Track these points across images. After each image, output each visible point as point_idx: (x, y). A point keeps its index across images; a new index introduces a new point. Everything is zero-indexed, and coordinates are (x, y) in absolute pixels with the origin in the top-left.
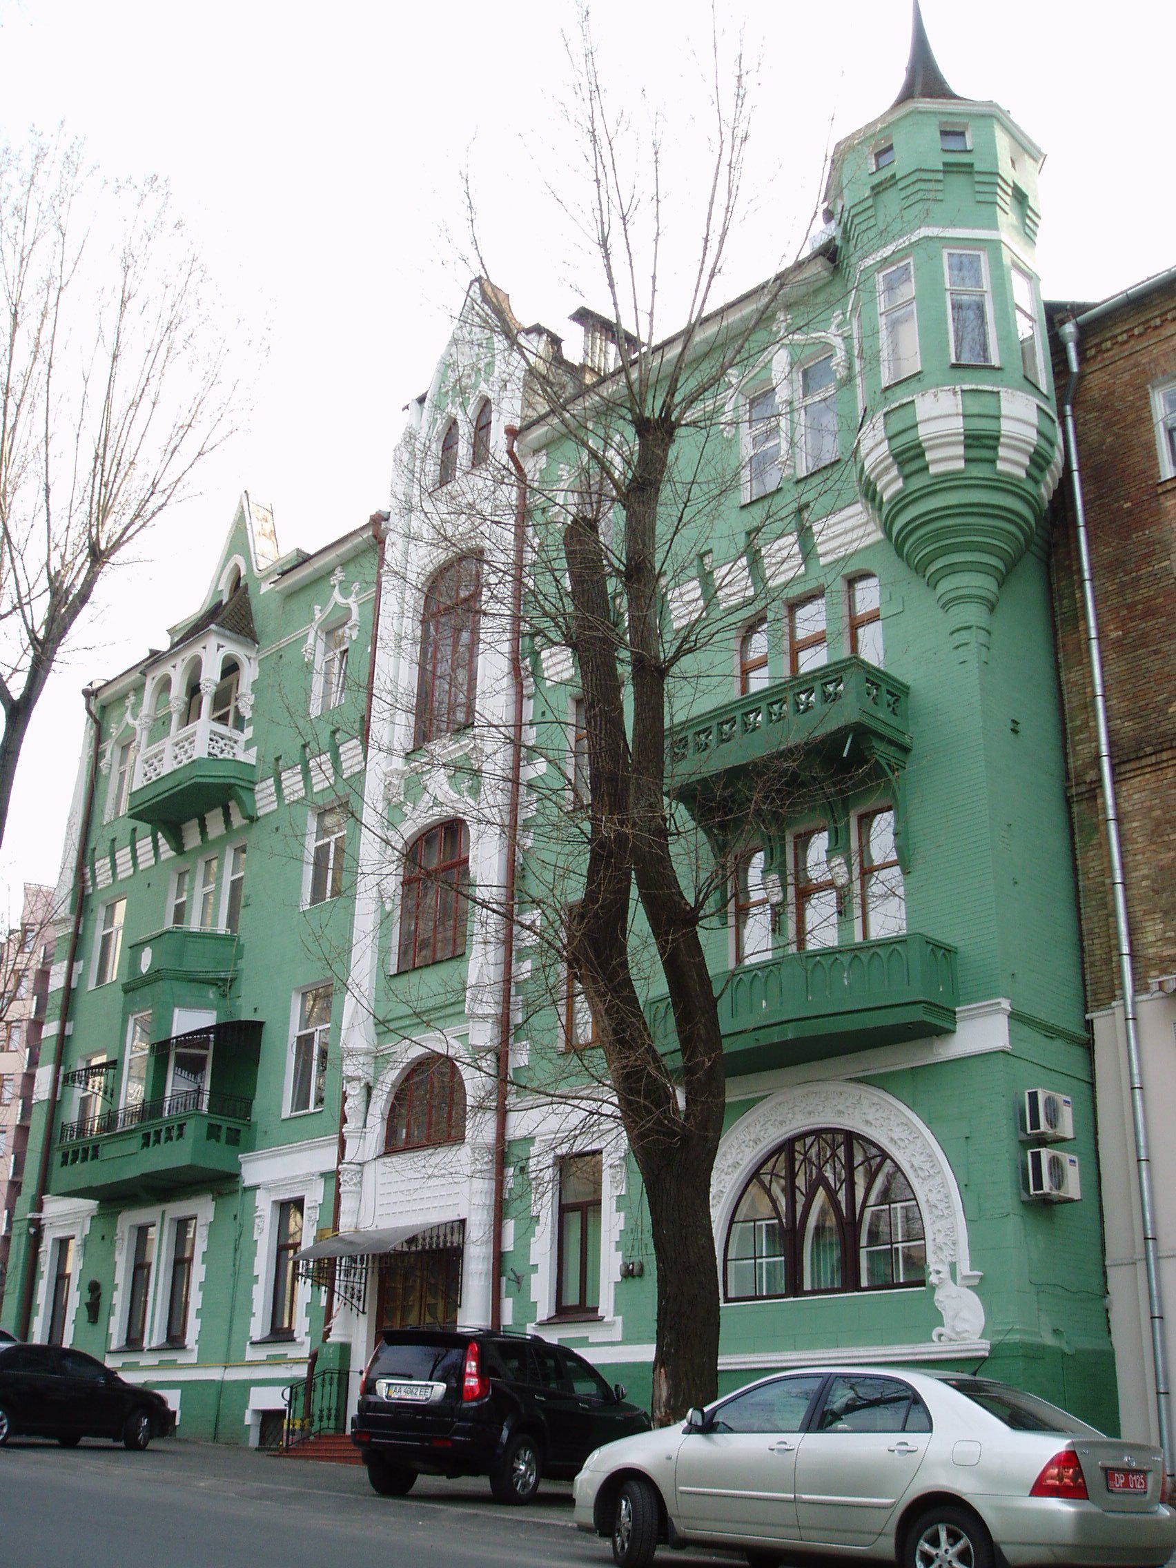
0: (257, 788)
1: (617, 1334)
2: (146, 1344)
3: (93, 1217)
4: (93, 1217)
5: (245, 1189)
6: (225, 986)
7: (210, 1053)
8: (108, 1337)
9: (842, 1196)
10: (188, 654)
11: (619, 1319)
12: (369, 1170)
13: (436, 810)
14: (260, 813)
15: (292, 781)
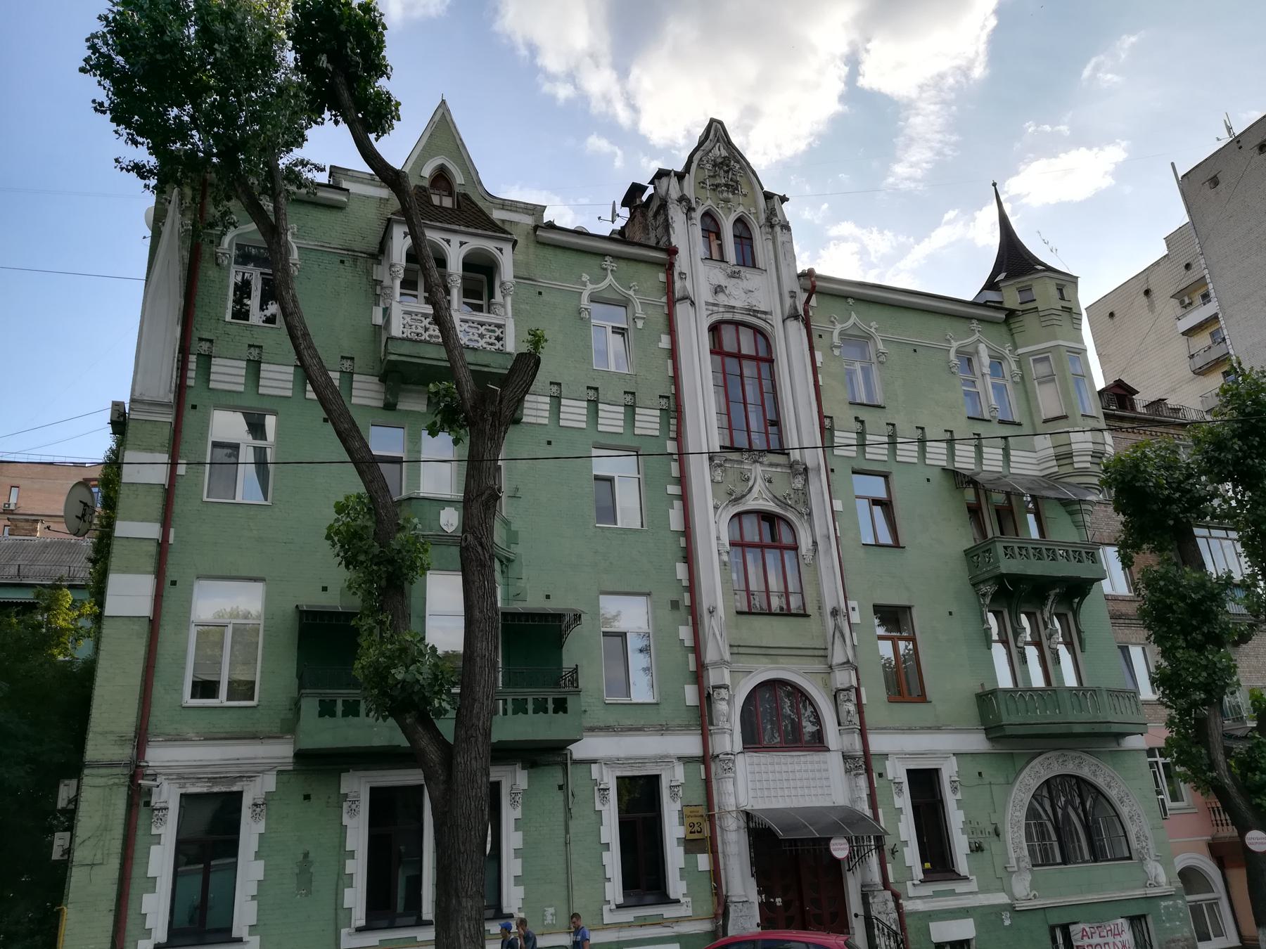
0: (527, 397)
1: (973, 886)
3: (280, 773)
4: (280, 773)
8: (340, 914)
9: (1080, 811)
10: (474, 243)
11: (973, 877)
13: (761, 501)
15: (574, 413)
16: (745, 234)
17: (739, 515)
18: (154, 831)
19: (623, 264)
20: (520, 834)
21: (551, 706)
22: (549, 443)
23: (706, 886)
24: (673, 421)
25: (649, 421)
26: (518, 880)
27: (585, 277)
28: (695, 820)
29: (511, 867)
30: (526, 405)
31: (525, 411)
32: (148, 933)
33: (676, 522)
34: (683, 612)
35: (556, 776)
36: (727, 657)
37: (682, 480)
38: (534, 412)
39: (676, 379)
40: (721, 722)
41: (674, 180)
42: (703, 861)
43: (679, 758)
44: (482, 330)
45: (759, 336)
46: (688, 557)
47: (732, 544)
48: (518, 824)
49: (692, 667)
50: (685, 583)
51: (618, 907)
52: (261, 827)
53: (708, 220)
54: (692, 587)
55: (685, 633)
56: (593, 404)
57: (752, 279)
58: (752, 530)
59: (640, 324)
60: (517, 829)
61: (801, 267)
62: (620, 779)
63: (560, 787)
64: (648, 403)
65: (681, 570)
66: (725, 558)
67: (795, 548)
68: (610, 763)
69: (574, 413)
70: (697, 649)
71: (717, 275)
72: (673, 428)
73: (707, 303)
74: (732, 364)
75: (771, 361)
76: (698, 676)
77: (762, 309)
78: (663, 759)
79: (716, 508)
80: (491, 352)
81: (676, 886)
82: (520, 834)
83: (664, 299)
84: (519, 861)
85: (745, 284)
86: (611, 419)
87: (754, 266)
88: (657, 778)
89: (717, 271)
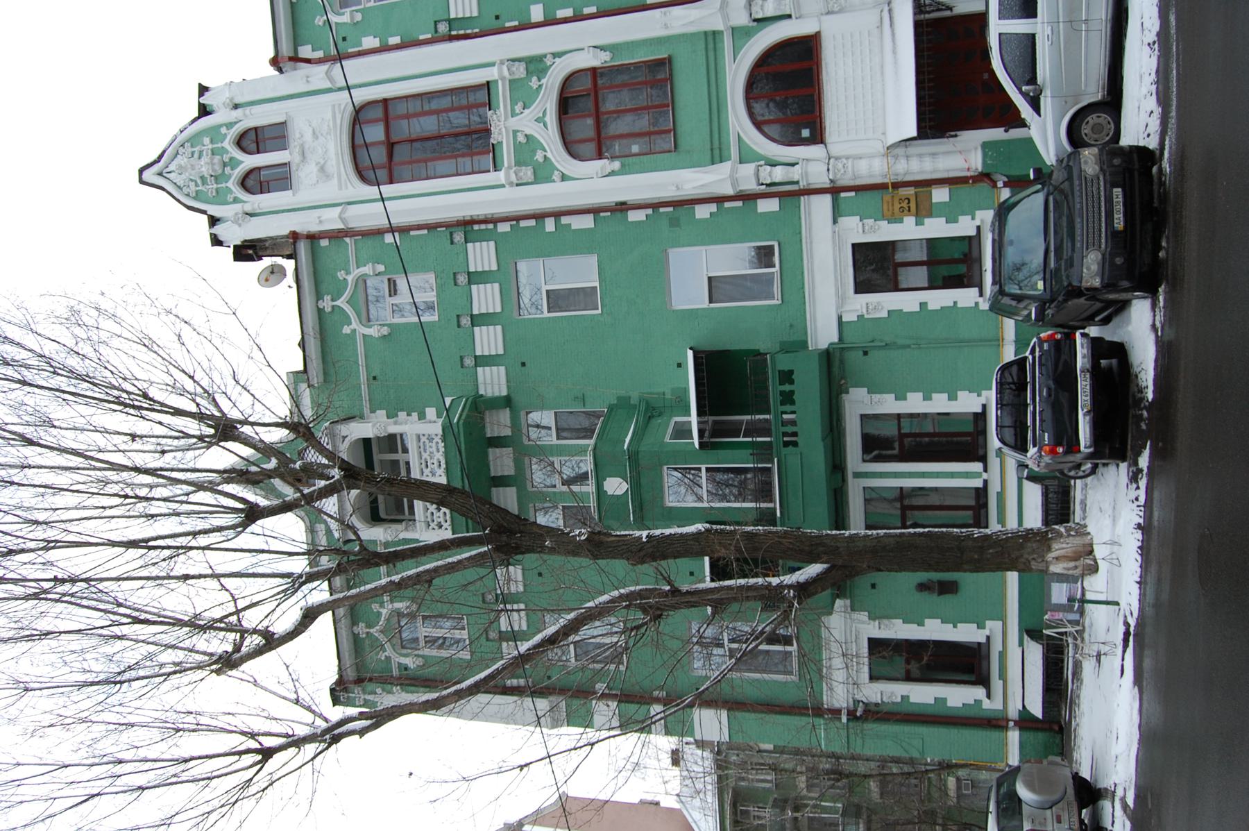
0: (482, 392)
2: (978, 483)
5: (840, 339)
6: (651, 411)
7: (712, 418)
12: (835, 149)
13: (547, 119)
14: (504, 393)
15: (488, 340)
16: (252, 135)
17: (570, 146)
18: (899, 700)
19: (323, 287)
20: (909, 395)
21: (787, 388)
22: (523, 364)
23: (964, 190)
24: (476, 227)
25: (482, 256)
26: (953, 397)
27: (346, 330)
28: (897, 206)
29: (939, 404)
30: (490, 394)
31: (497, 394)
32: (978, 702)
33: (587, 222)
34: (682, 211)
35: (854, 358)
36: (726, 167)
37: (540, 216)
38: (496, 387)
39: (432, 227)
40: (795, 173)
41: (218, 230)
42: (940, 195)
43: (835, 222)
44: (425, 456)
45: (362, 116)
46: (622, 207)
47: (600, 156)
48: (901, 397)
49: (740, 204)
50: (650, 211)
51: (981, 295)
52: (898, 622)
53: (250, 183)
54: (656, 206)
55: (703, 212)
56: (477, 320)
57: (300, 131)
58: (584, 127)
59: (381, 268)
60: (905, 399)
61: (272, 71)
62: (856, 292)
63: (866, 353)
64: (461, 257)
65: (635, 216)
66: (616, 165)
67: (594, 70)
68: (841, 300)
69: (488, 340)
70: (719, 200)
71: (305, 175)
72: (483, 227)
73: (340, 188)
74: (401, 152)
75: (385, 102)
76: (748, 198)
77: (329, 116)
78: (837, 238)
79: (564, 178)
80: (445, 447)
81: (964, 227)
82: (909, 395)
83: (347, 240)
84: (934, 396)
85: (308, 137)
86: (486, 298)
87: (283, 124)
88: (853, 245)
89: (302, 174)
